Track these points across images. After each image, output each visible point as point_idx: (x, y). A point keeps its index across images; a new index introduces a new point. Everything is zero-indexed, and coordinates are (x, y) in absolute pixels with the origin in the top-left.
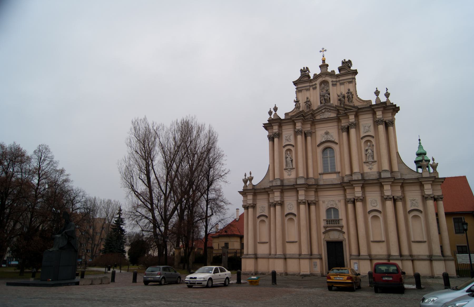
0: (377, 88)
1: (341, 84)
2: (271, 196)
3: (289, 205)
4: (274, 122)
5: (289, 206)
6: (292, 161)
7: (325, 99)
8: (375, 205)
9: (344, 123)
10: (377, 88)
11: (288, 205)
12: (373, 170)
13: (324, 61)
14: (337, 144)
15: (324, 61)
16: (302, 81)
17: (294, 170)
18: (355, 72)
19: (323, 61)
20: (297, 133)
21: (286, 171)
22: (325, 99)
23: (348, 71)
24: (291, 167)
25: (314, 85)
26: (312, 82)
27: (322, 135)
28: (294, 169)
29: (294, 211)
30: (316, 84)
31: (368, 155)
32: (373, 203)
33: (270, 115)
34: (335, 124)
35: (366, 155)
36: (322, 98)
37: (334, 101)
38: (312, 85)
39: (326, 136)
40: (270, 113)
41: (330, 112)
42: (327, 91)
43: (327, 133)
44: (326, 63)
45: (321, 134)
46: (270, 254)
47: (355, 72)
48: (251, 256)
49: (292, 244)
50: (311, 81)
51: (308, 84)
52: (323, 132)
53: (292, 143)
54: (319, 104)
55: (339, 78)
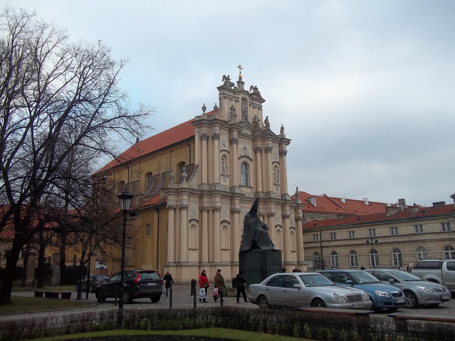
0: (282, 125)
1: (254, 107)
2: (206, 200)
3: (224, 212)
4: (220, 122)
5: (224, 213)
6: (227, 167)
7: (245, 116)
8: (279, 221)
9: (259, 144)
10: (282, 125)
11: (223, 213)
12: (278, 192)
13: (240, 78)
14: (251, 160)
15: (240, 78)
16: (227, 88)
17: (228, 177)
18: (263, 101)
19: (239, 77)
20: (232, 141)
21: (223, 176)
22: (245, 116)
23: (259, 97)
24: (226, 174)
25: (236, 97)
26: (235, 94)
27: (242, 149)
28: (228, 176)
29: (228, 219)
30: (239, 98)
31: (276, 178)
32: (278, 219)
33: (204, 111)
34: (250, 142)
35: (274, 177)
36: (243, 114)
37: (250, 120)
38: (235, 97)
39: (244, 151)
40: (204, 108)
41: (248, 129)
42: (246, 108)
43: (245, 148)
44: (243, 80)
45: (241, 148)
46: (200, 262)
47: (263, 101)
48: (186, 264)
49: (225, 251)
50: (235, 92)
51: (232, 94)
52: (243, 146)
53: (227, 149)
54: (241, 119)
55: (253, 101)
